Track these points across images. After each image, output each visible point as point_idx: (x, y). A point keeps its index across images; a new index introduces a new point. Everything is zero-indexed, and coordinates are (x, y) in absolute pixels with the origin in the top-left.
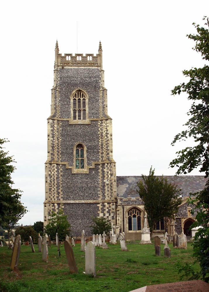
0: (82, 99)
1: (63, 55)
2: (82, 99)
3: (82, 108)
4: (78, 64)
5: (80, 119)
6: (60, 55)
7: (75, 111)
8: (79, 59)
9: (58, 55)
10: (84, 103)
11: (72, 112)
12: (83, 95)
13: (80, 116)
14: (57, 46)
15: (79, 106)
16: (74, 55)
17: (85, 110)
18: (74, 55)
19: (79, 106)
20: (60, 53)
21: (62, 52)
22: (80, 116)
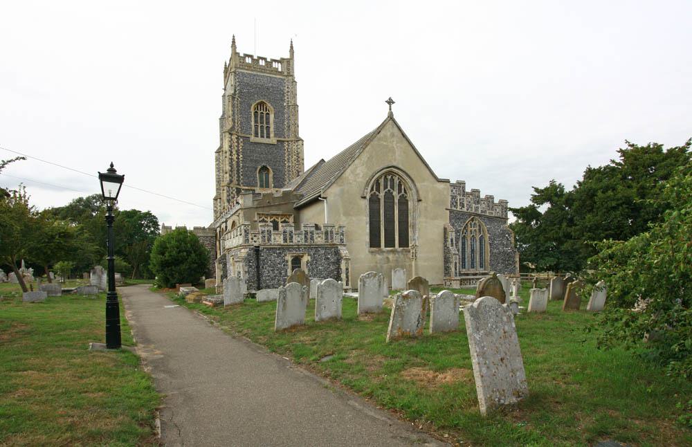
0: (265, 113)
1: (242, 55)
2: (265, 113)
3: (265, 125)
4: (262, 69)
5: (262, 137)
6: (239, 54)
7: (256, 126)
8: (262, 63)
9: (235, 53)
10: (268, 119)
11: (253, 128)
12: (266, 108)
13: (262, 132)
14: (234, 42)
15: (262, 123)
16: (255, 57)
17: (268, 128)
18: (255, 57)
19: (262, 123)
20: (237, 51)
21: (241, 51)
22: (262, 132)
